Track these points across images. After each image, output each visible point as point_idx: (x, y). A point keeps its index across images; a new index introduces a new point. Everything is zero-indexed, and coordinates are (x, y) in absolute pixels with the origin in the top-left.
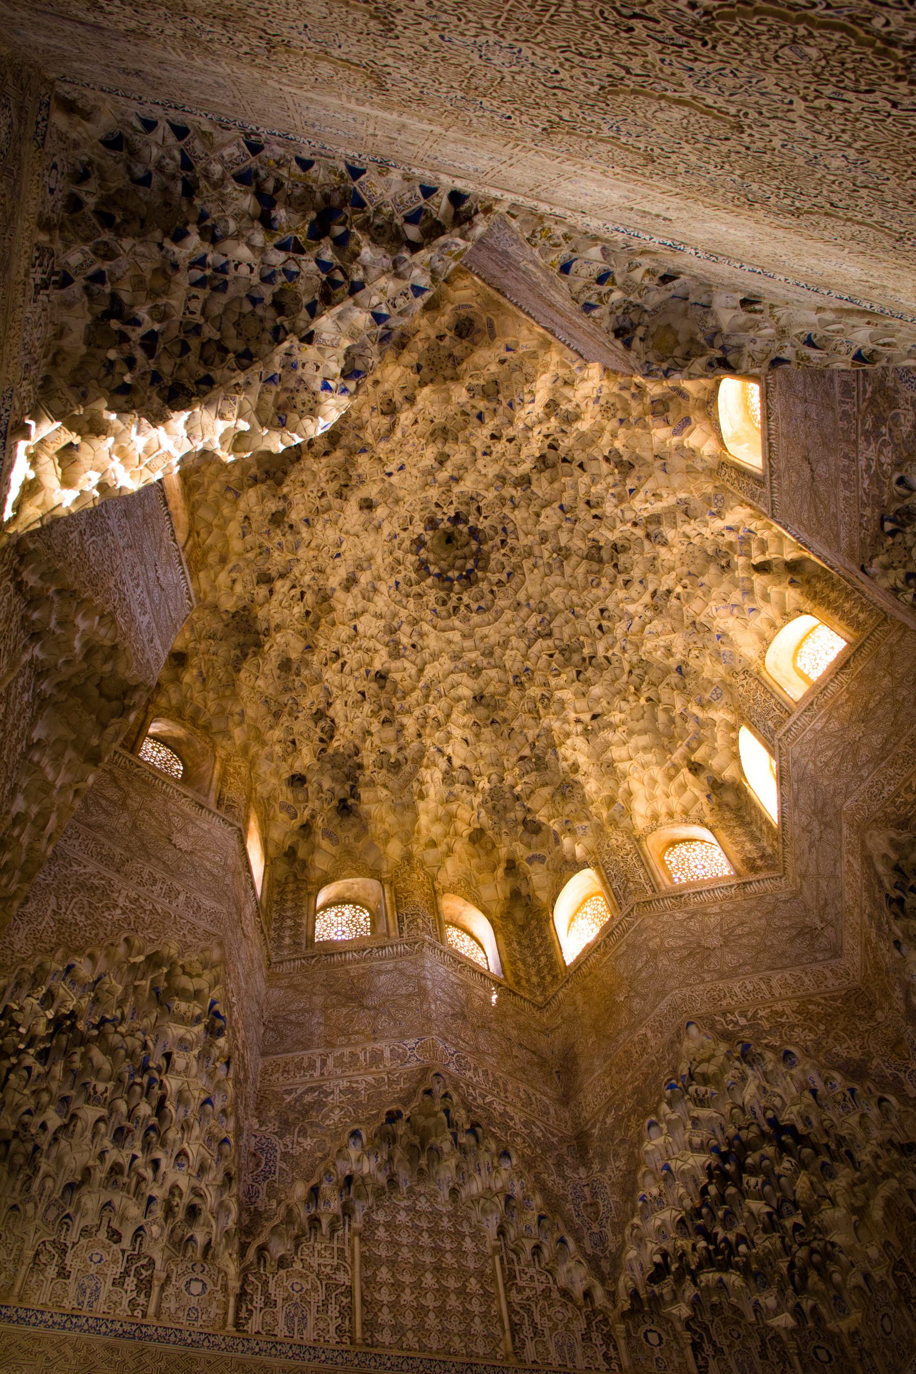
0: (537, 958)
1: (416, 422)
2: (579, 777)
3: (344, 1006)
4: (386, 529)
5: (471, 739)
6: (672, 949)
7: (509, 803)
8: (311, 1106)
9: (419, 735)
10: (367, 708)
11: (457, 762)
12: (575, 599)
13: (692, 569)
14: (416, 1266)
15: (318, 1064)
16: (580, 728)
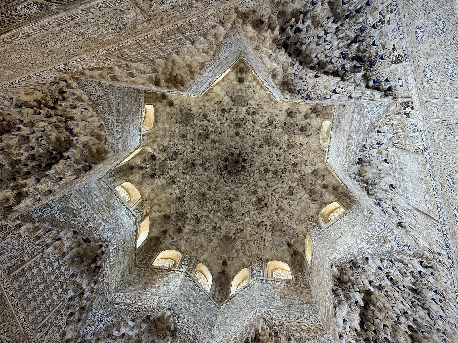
0: (146, 256)
1: (269, 133)
2: (202, 233)
3: (106, 206)
4: (233, 143)
5: (192, 199)
6: (182, 290)
7: (181, 220)
8: (73, 214)
9: (186, 184)
10: (184, 166)
11: (184, 199)
12: (246, 203)
13: (275, 228)
14: (44, 279)
15: (86, 209)
16: (214, 225)
